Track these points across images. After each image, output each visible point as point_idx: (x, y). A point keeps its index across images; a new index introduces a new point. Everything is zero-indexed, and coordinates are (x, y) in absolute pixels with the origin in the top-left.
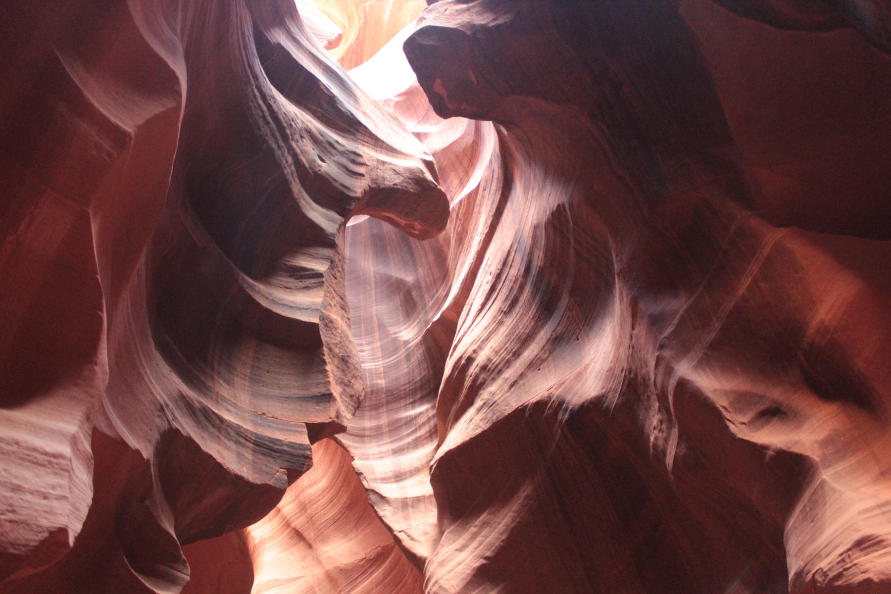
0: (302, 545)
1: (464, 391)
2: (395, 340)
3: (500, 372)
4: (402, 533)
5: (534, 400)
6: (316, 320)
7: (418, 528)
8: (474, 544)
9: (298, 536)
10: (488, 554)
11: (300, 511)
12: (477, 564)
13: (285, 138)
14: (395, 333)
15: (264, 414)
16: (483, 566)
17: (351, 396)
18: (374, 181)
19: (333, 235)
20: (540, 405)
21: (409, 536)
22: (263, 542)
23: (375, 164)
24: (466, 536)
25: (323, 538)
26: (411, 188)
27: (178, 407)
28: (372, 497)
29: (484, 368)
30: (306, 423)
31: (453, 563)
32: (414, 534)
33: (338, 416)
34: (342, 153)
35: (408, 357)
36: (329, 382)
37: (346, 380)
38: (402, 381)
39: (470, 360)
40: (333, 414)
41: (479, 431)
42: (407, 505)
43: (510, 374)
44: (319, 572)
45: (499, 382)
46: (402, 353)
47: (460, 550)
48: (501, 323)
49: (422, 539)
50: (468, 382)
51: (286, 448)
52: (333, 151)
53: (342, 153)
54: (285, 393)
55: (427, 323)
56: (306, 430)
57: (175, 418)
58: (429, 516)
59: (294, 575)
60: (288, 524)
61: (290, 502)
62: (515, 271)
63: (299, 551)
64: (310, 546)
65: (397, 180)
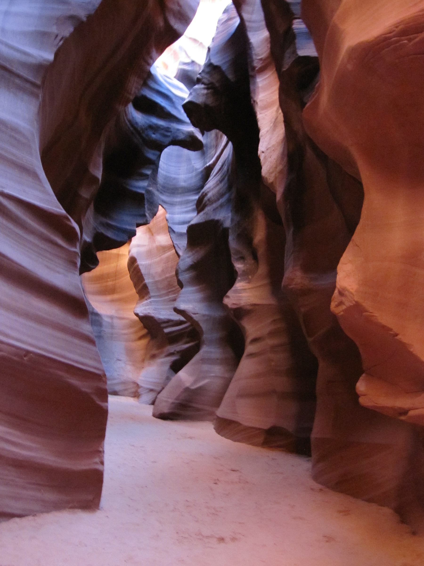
2: (193, 167)
3: (212, 203)
6: (143, 192)
10: (195, 261)
12: (191, 263)
14: (194, 164)
16: (193, 265)
18: (173, 138)
20: (218, 221)
25: (158, 234)
29: (209, 200)
32: (179, 246)
33: (147, 221)
34: (162, 129)
35: (196, 175)
39: (206, 194)
40: (145, 220)
41: (201, 221)
42: (181, 235)
43: (215, 205)
46: (194, 174)
47: (189, 257)
49: (182, 248)
53: (162, 129)
55: (206, 163)
58: (183, 243)
64: (153, 235)
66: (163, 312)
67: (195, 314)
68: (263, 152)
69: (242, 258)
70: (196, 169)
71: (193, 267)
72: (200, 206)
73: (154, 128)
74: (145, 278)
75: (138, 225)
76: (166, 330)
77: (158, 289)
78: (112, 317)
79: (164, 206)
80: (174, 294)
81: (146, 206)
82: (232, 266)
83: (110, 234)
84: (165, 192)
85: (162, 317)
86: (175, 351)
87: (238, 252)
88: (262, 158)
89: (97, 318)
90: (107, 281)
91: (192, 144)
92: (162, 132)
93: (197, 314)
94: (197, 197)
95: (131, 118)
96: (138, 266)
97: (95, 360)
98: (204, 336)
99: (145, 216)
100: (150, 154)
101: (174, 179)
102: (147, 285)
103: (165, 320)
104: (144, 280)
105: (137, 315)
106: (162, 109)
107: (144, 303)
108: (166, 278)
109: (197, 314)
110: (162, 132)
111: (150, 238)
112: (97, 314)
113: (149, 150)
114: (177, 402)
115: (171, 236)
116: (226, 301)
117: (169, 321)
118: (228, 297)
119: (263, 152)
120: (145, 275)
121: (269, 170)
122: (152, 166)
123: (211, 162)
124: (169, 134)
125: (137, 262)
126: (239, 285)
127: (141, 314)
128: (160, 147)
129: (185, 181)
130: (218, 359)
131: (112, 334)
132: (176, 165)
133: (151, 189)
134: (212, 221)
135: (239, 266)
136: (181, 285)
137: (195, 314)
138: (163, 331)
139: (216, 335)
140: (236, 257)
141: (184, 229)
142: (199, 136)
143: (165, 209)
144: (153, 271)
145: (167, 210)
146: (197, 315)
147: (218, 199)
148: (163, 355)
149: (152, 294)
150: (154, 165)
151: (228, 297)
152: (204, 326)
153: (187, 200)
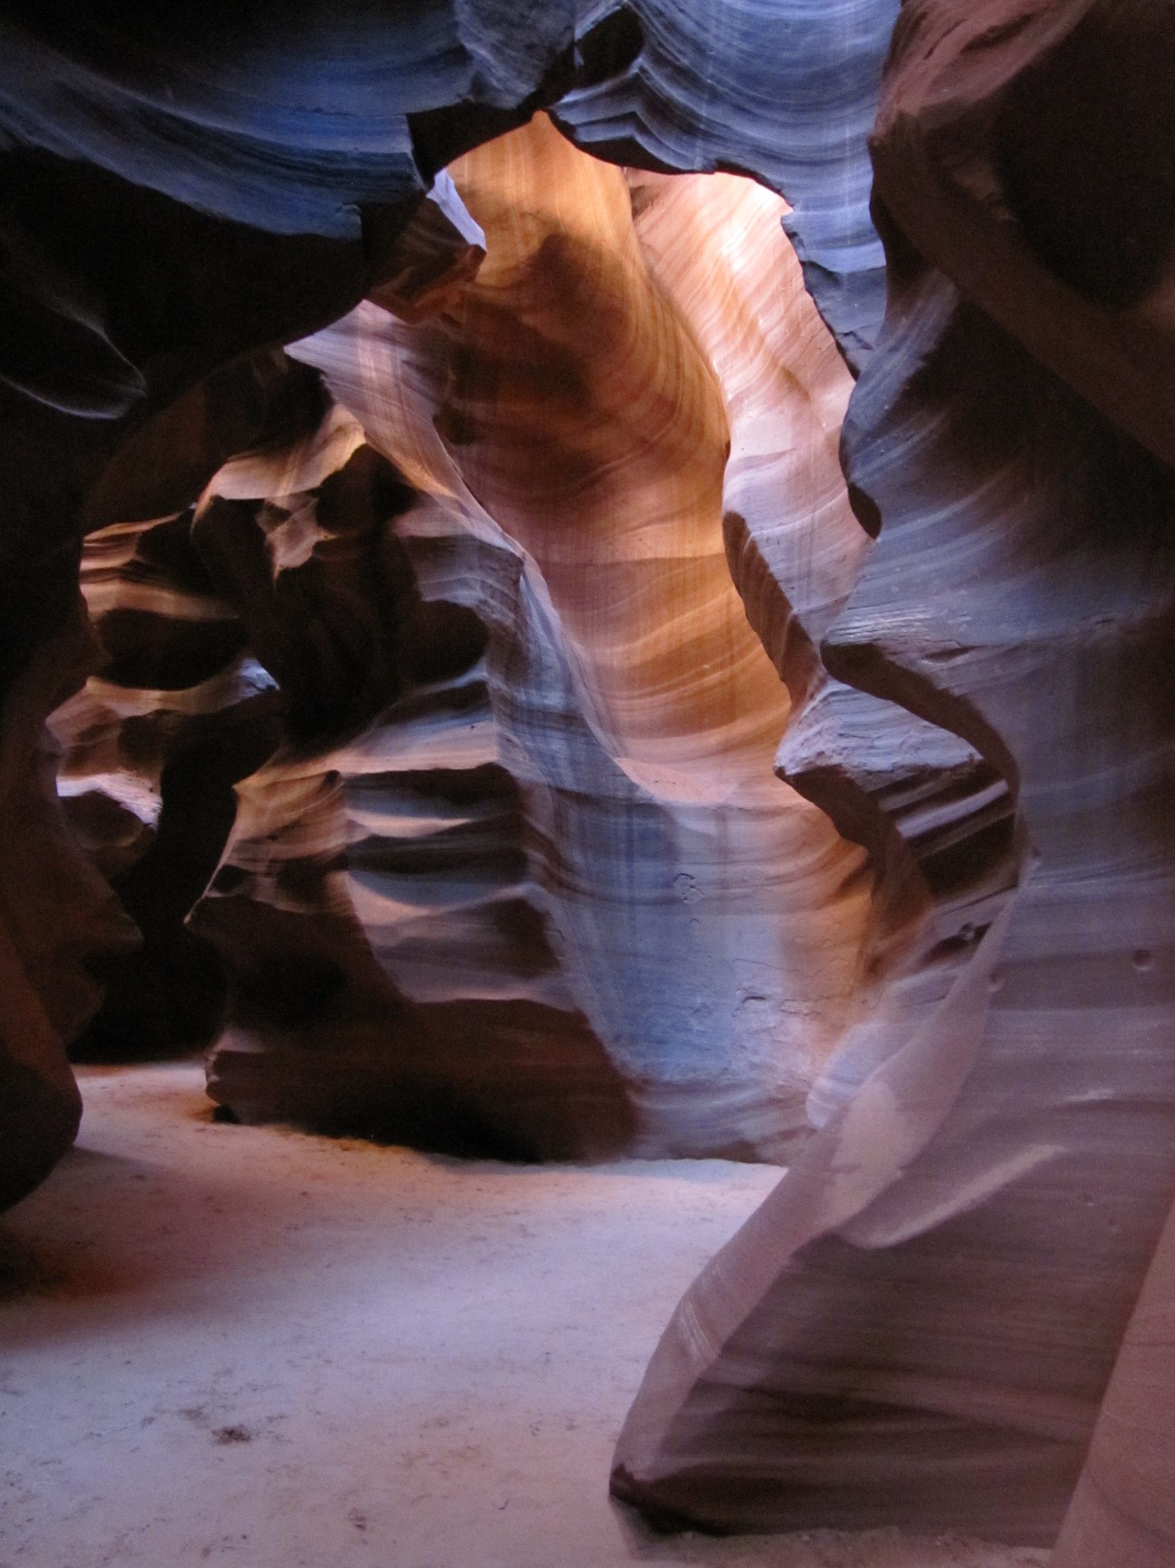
4: (851, 338)
11: (792, 335)
12: (912, 371)
15: (319, 110)
17: (530, 47)
21: (860, 341)
22: (739, 398)
30: (409, 115)
31: (878, 376)
33: (479, 86)
36: (456, 25)
37: (512, 14)
47: (894, 350)
51: (355, 166)
56: (406, 127)
59: (779, 450)
61: (777, 324)
64: (806, 396)
66: (889, 739)
71: (921, 391)
74: (791, 594)
76: (910, 827)
78: (720, 814)
84: (763, 104)
85: (880, 763)
86: (966, 927)
89: (651, 824)
90: (703, 674)
93: (964, 650)
96: (754, 548)
99: (460, 56)
101: (805, 27)
102: (804, 624)
103: (900, 776)
109: (964, 650)
111: (797, 418)
112: (650, 809)
114: (748, 1373)
117: (920, 775)
120: (789, 580)
125: (749, 534)
129: (865, 26)
130: (1141, 956)
131: (724, 884)
138: (898, 834)
139: (1107, 777)
143: (778, 192)
144: (822, 558)
145: (793, 195)
146: (960, 660)
148: (911, 959)
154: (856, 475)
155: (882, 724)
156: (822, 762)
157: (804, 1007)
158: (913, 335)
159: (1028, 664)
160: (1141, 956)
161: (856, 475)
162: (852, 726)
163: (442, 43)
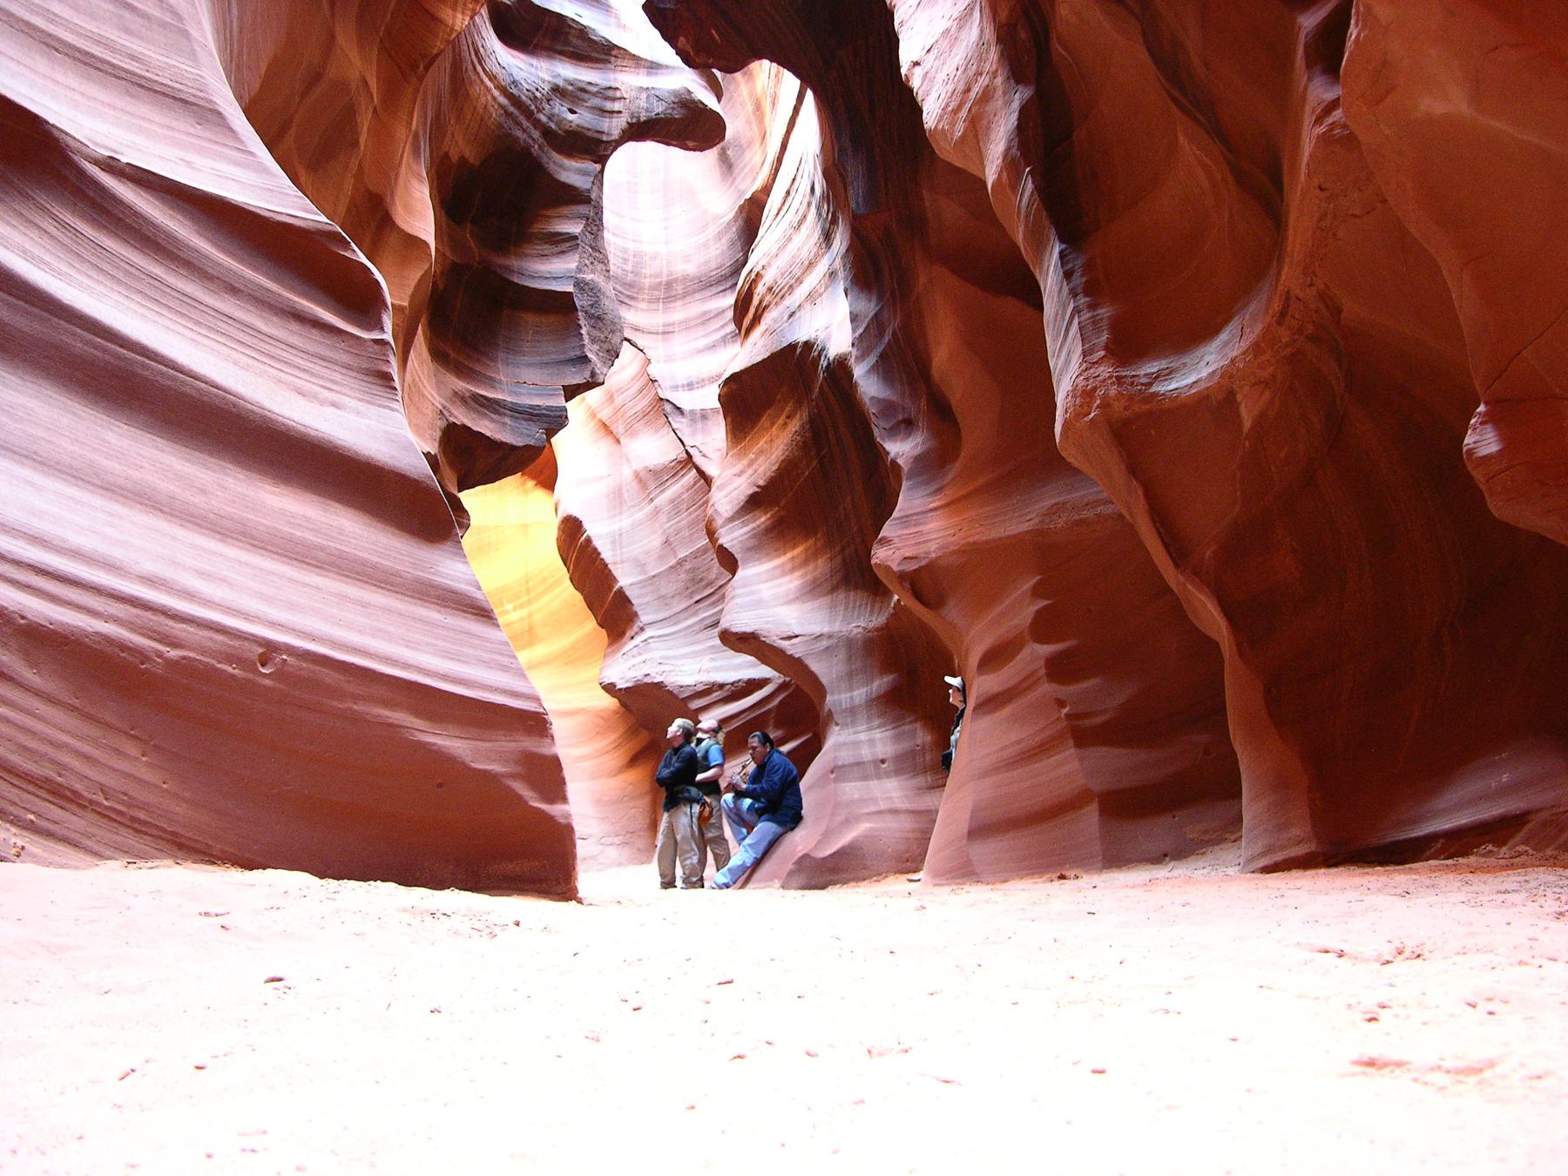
0: (610, 440)
1: (752, 310)
5: (804, 339)
6: (570, 289)
7: (711, 441)
8: (750, 471)
9: (605, 428)
10: (761, 483)
13: (529, 115)
19: (589, 191)
20: (808, 345)
23: (634, 94)
24: (745, 462)
26: (678, 114)
27: (453, 403)
28: (668, 407)
29: (770, 289)
31: (730, 488)
33: (593, 374)
34: (595, 95)
35: (719, 236)
38: (714, 265)
40: (587, 374)
44: (627, 473)
45: (781, 307)
46: (712, 231)
47: (740, 474)
48: (790, 239)
50: (755, 302)
52: (586, 96)
53: (595, 95)
54: (545, 359)
55: (744, 193)
57: (451, 414)
60: (593, 415)
62: (803, 186)
63: (605, 445)
64: (618, 441)
65: (659, 108)
67: (790, 638)
68: (917, 64)
69: (906, 426)
70: (717, 217)
71: (754, 503)
72: (746, 314)
73: (571, 94)
74: (617, 571)
75: (571, 392)
77: (663, 600)
79: (640, 343)
80: (714, 604)
81: (583, 331)
82: (878, 453)
83: (485, 426)
87: (887, 408)
88: (915, 83)
91: (691, 127)
92: (596, 101)
94: (730, 299)
95: (496, 70)
96: (589, 540)
97: (505, 669)
98: (829, 698)
99: (584, 359)
100: (572, 172)
102: (628, 593)
103: (700, 688)
104: (615, 580)
105: (610, 688)
106: (583, 32)
107: (626, 649)
108: (681, 563)
110: (596, 101)
113: (567, 162)
115: (675, 426)
116: (880, 555)
118: (886, 541)
119: (917, 64)
121: (947, 105)
122: (582, 209)
123: (757, 185)
124: (617, 106)
126: (908, 500)
127: (621, 685)
128: (596, 149)
129: (687, 259)
130: (883, 761)
132: (653, 208)
133: (589, 277)
134: (792, 347)
135: (901, 449)
136: (729, 562)
137: (790, 638)
140: (882, 424)
141: (710, 398)
142: (709, 100)
144: (636, 549)
147: (799, 281)
149: (644, 618)
150: (585, 201)
151: (886, 541)
152: (822, 669)
153: (705, 313)
154: (721, 541)
155: (684, 656)
156: (648, 680)
157: (617, 840)
158: (750, 471)
159: (825, 643)
160: (883, 761)
161: (721, 541)
162: (667, 658)
163: (578, 353)
